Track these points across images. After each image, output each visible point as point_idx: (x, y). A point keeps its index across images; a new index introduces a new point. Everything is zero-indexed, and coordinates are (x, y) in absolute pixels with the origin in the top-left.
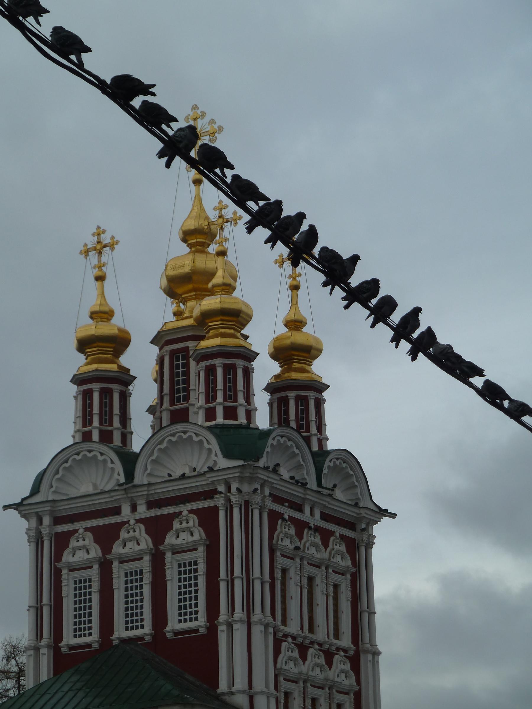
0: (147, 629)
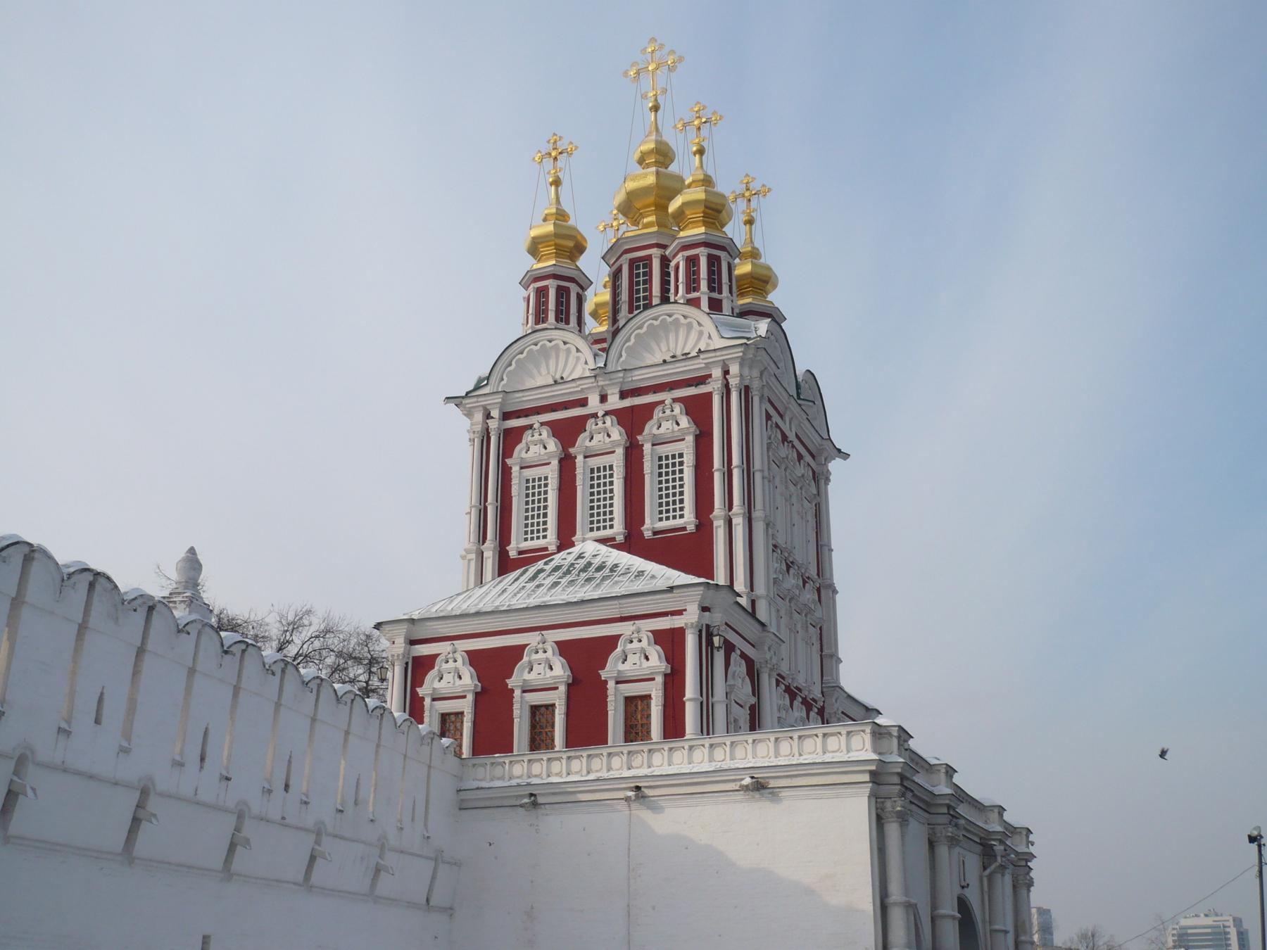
0: (618, 529)
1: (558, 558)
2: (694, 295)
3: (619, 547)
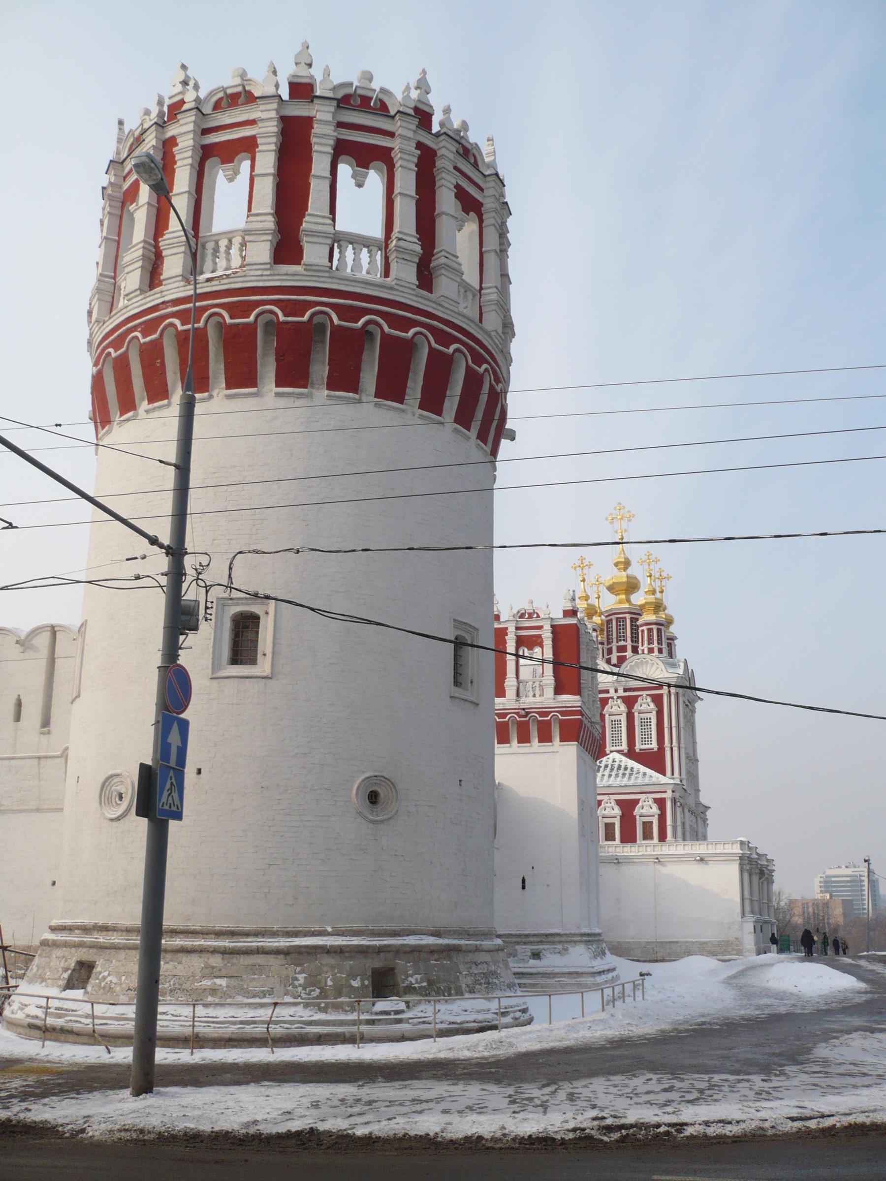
0: (624, 747)
1: (604, 759)
2: (651, 646)
3: (624, 755)
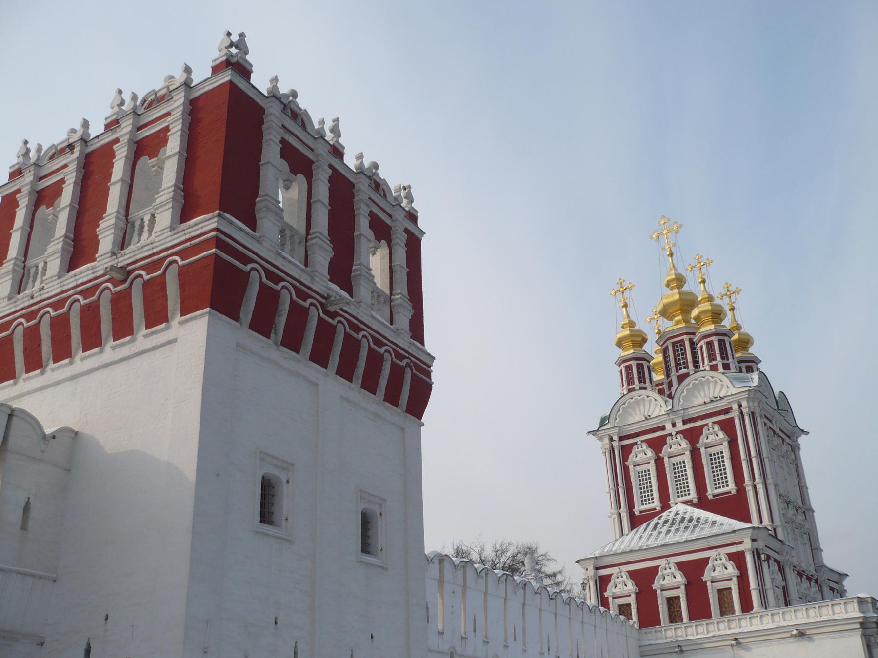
0: (693, 495)
1: (665, 514)
2: (714, 363)
3: (695, 505)
